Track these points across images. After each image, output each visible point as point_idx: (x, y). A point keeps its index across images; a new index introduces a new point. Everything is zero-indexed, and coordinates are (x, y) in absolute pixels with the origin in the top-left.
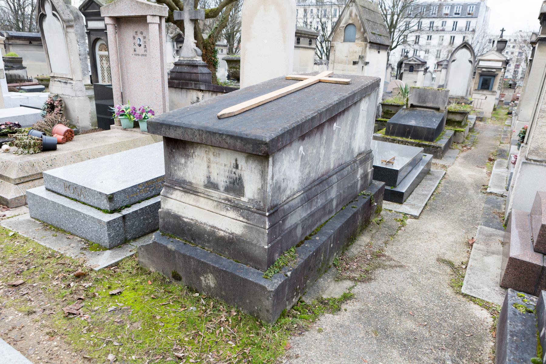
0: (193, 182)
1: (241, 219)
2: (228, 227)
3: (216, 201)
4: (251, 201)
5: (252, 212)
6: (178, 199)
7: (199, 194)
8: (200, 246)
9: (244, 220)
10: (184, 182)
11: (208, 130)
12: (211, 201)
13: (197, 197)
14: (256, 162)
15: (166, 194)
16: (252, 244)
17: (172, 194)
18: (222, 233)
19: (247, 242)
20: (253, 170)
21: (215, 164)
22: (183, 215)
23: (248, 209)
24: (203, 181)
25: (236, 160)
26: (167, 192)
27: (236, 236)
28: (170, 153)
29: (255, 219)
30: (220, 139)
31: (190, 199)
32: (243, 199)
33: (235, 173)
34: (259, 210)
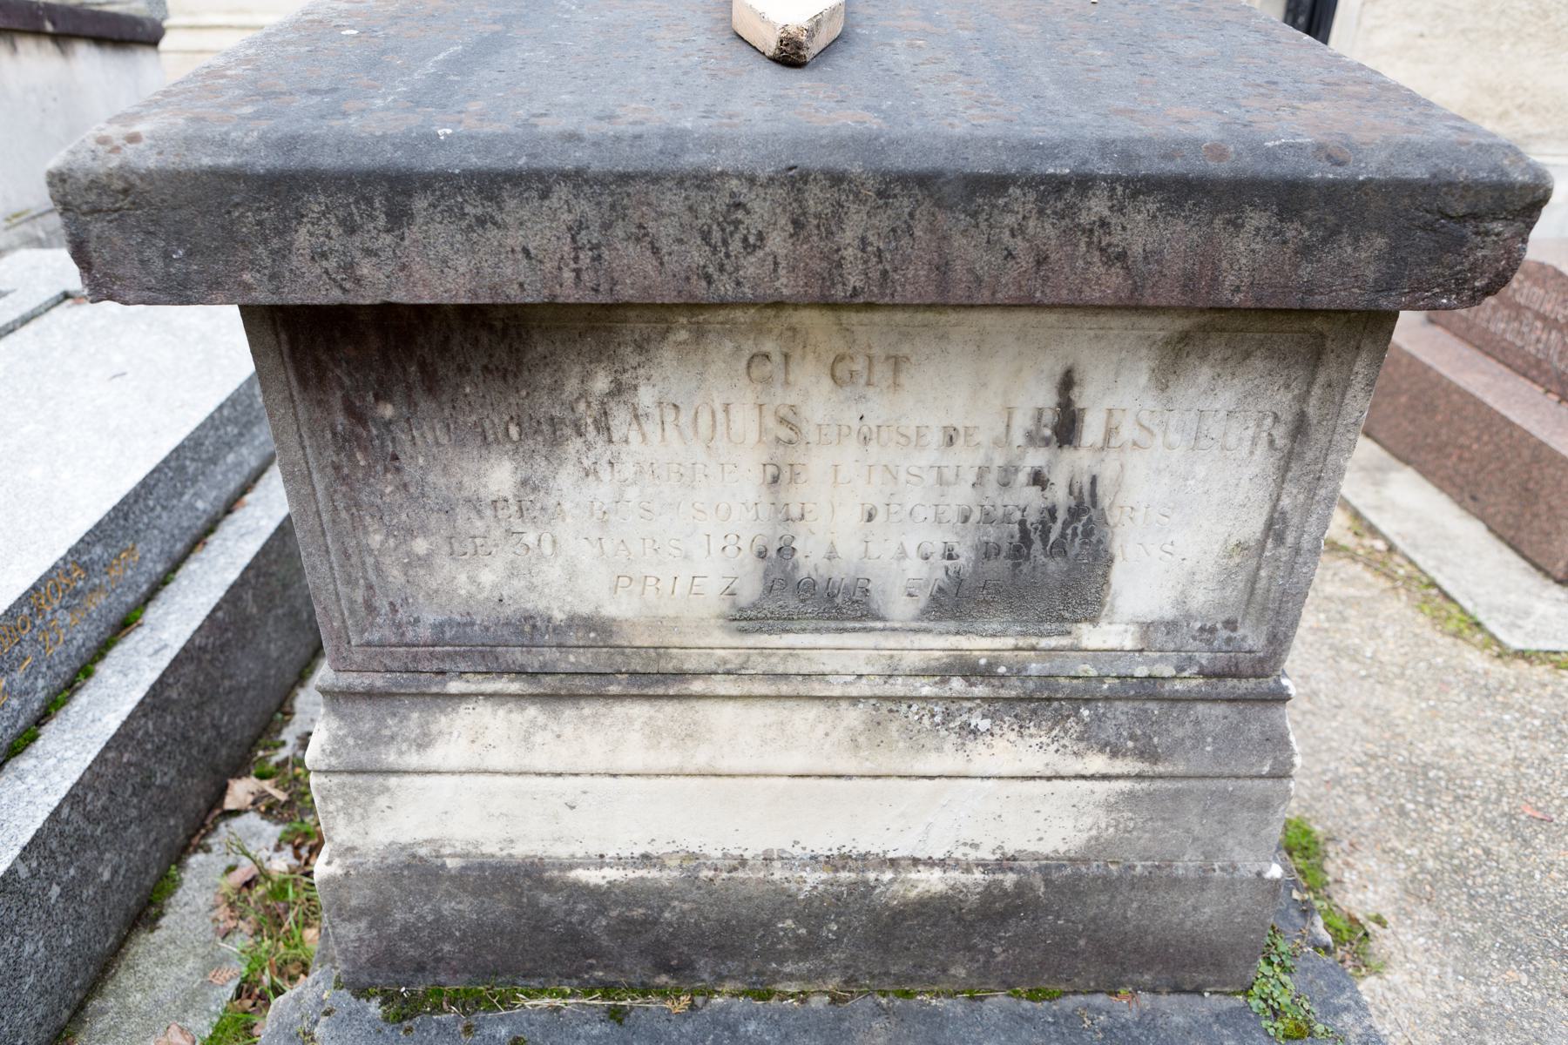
0: (610, 610)
1: (1097, 763)
2: (967, 835)
3: (855, 700)
4: (1159, 638)
5: (1175, 699)
6: (496, 760)
7: (697, 686)
8: (728, 986)
9: (1119, 766)
10: (530, 628)
11: (897, 161)
12: (812, 712)
13: (670, 708)
14: (1259, 363)
15: (363, 758)
16: (1175, 882)
17: (423, 742)
18: (932, 882)
19: (1145, 883)
20: (1214, 427)
21: (852, 447)
22: (561, 851)
23: (1148, 690)
24: (713, 586)
25: (1067, 383)
26: (374, 740)
27: (1045, 870)
28: (344, 442)
29: (1199, 739)
30: (1046, 231)
31: (623, 733)
32: (1092, 637)
33: (1038, 479)
34: (1220, 676)
